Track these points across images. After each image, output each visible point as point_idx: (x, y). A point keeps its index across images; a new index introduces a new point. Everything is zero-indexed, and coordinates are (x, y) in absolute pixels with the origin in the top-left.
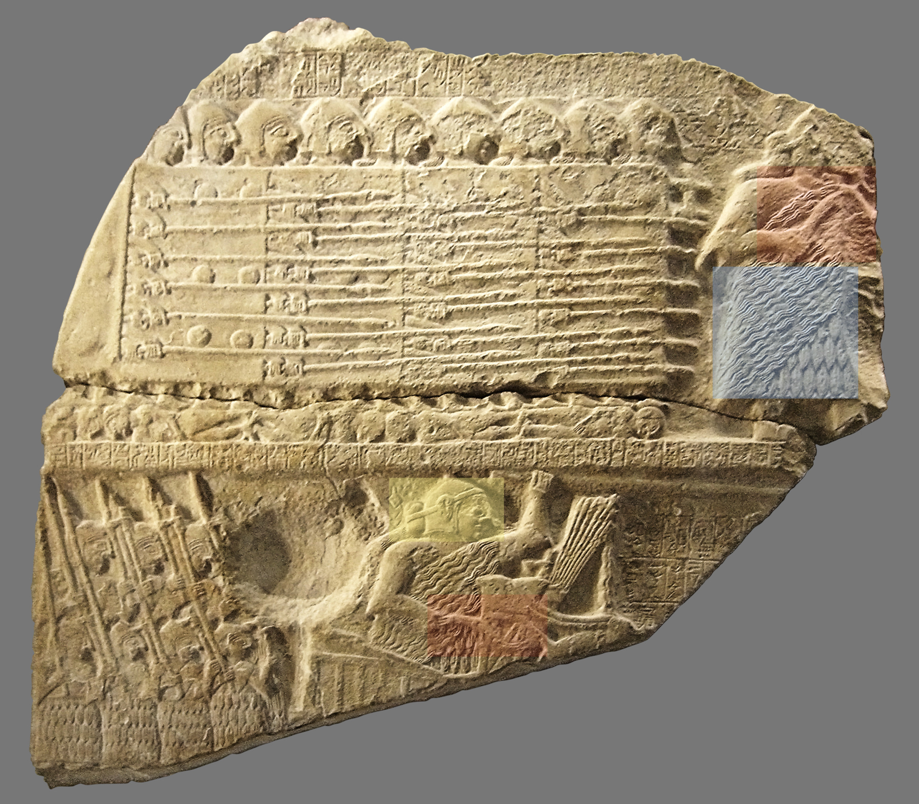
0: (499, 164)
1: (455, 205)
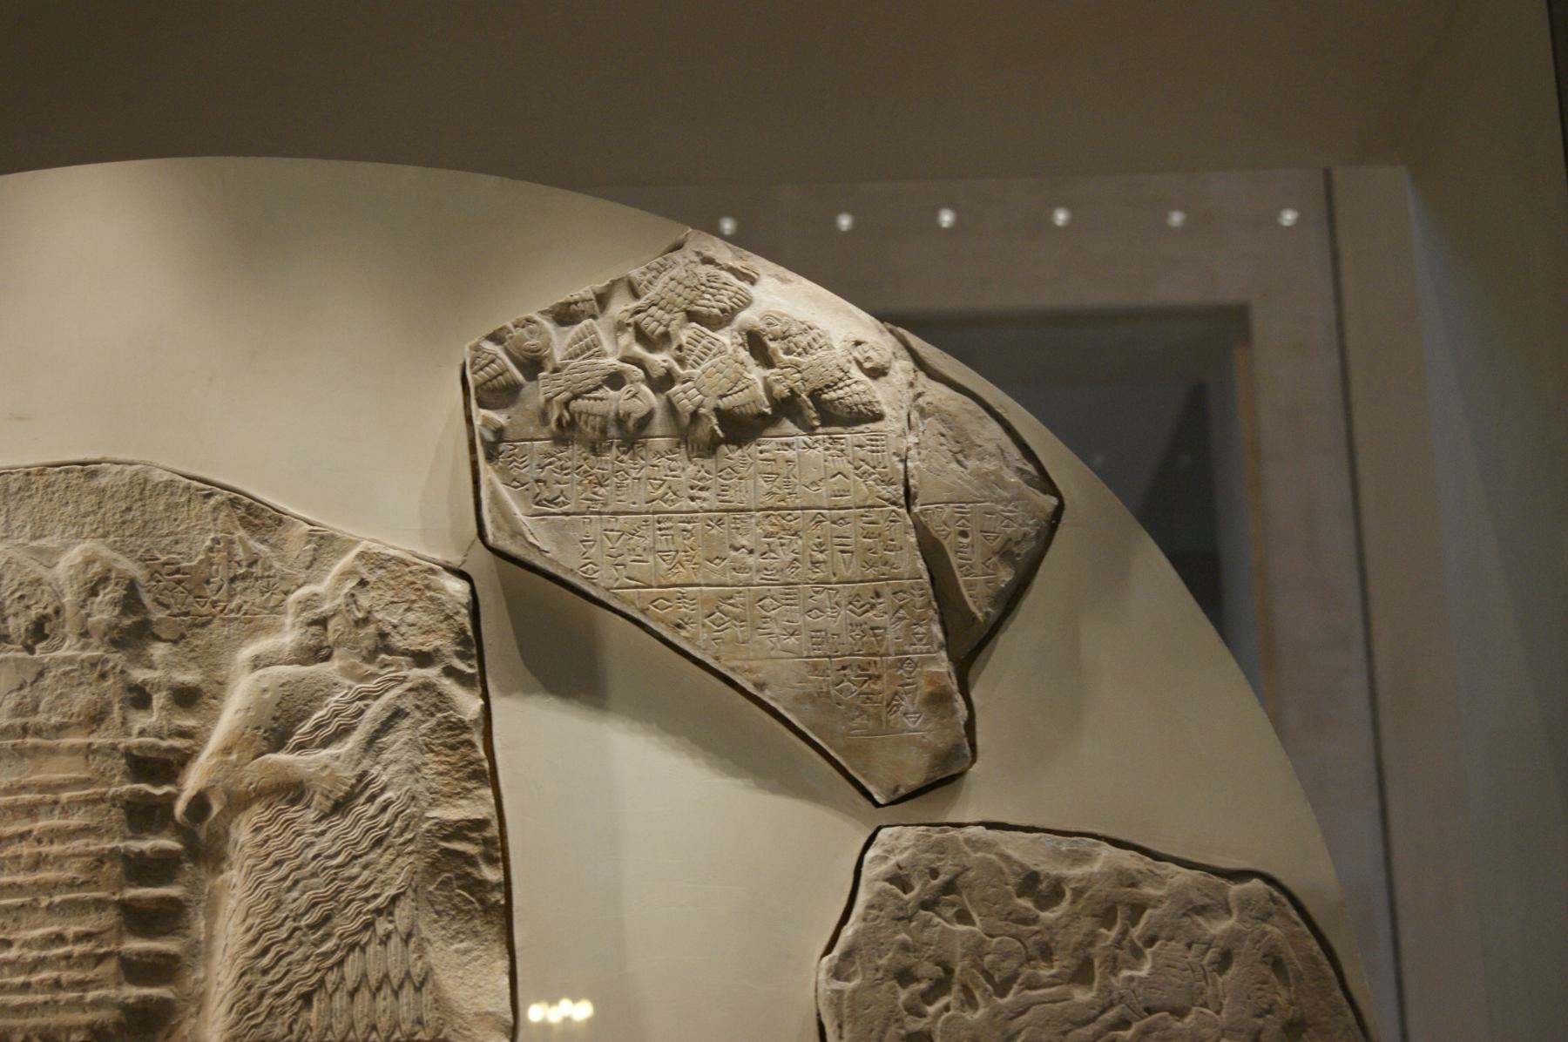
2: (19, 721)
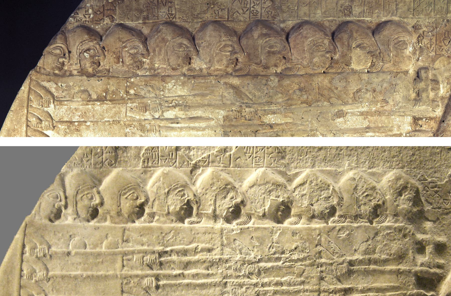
0: (291, 224)
1: (259, 257)
2: (367, 257)
